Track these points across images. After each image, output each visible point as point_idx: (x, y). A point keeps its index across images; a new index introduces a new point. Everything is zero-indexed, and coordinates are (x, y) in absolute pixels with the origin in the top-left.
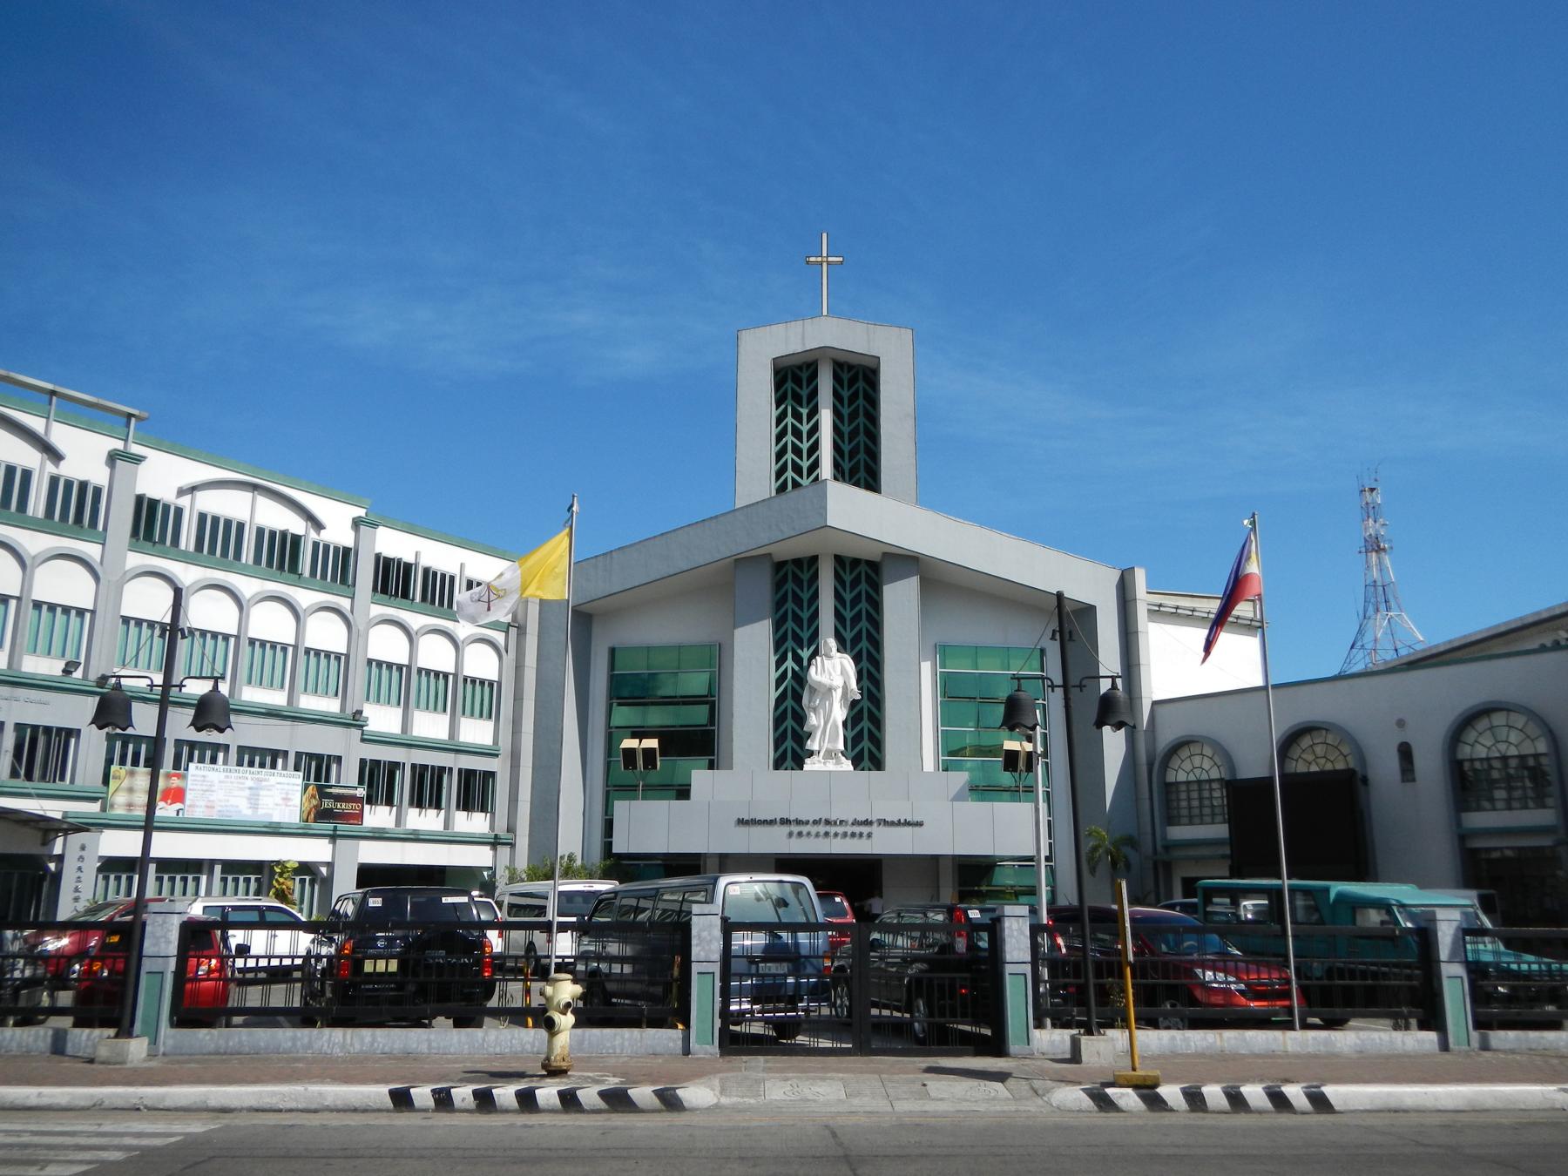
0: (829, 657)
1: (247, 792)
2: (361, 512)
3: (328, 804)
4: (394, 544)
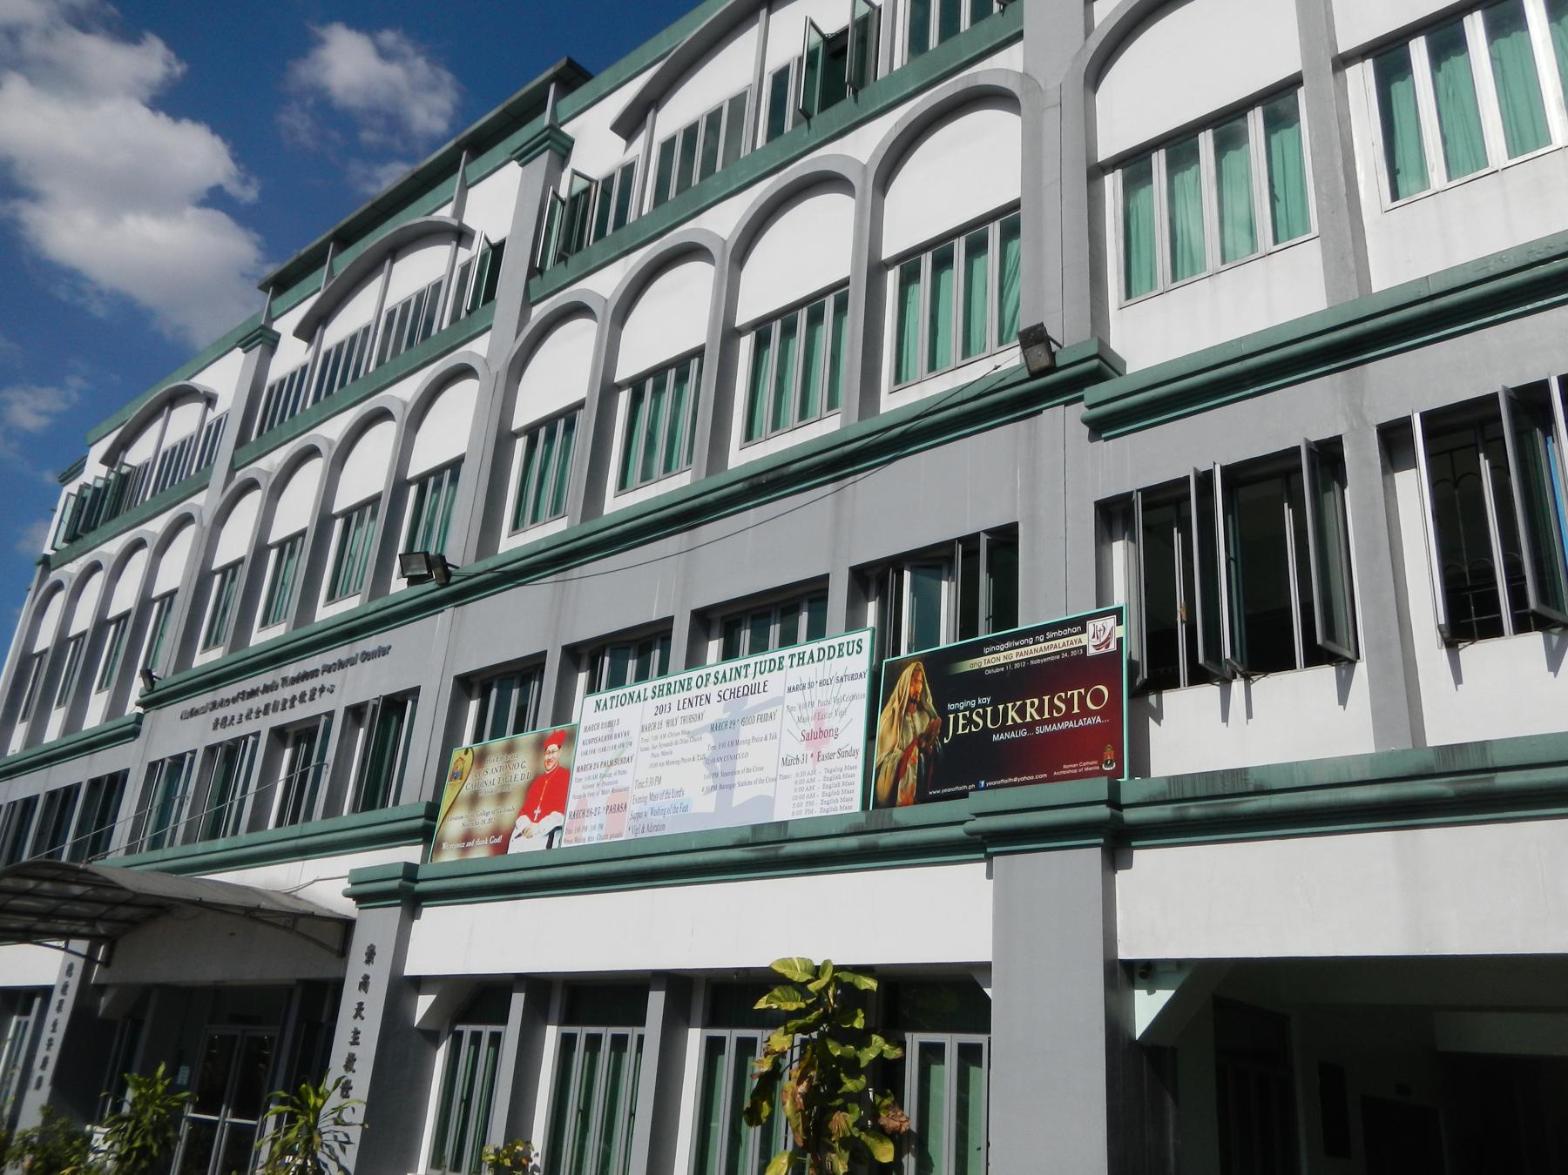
1: (708, 739)
3: (969, 716)
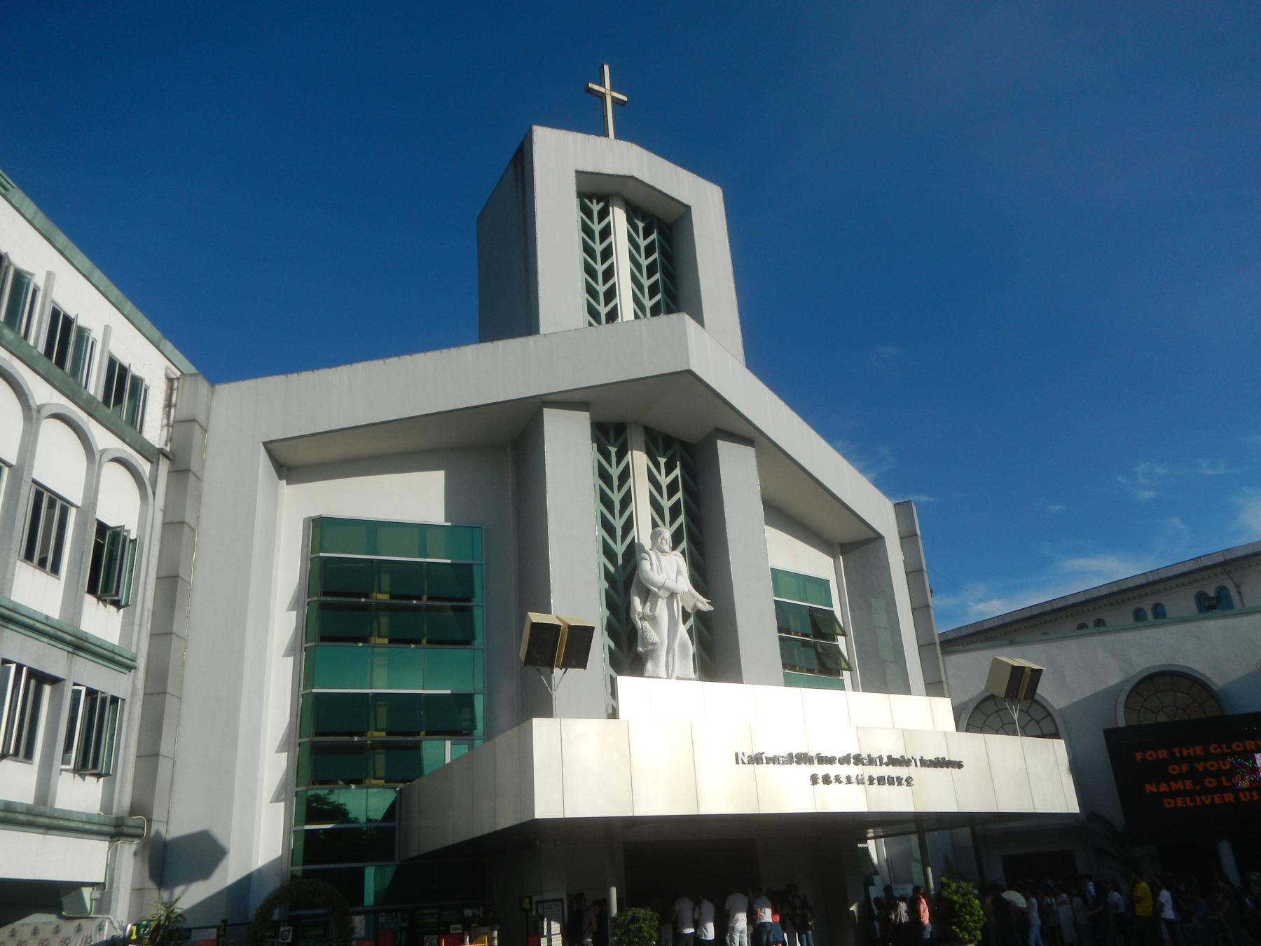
0: (663, 552)
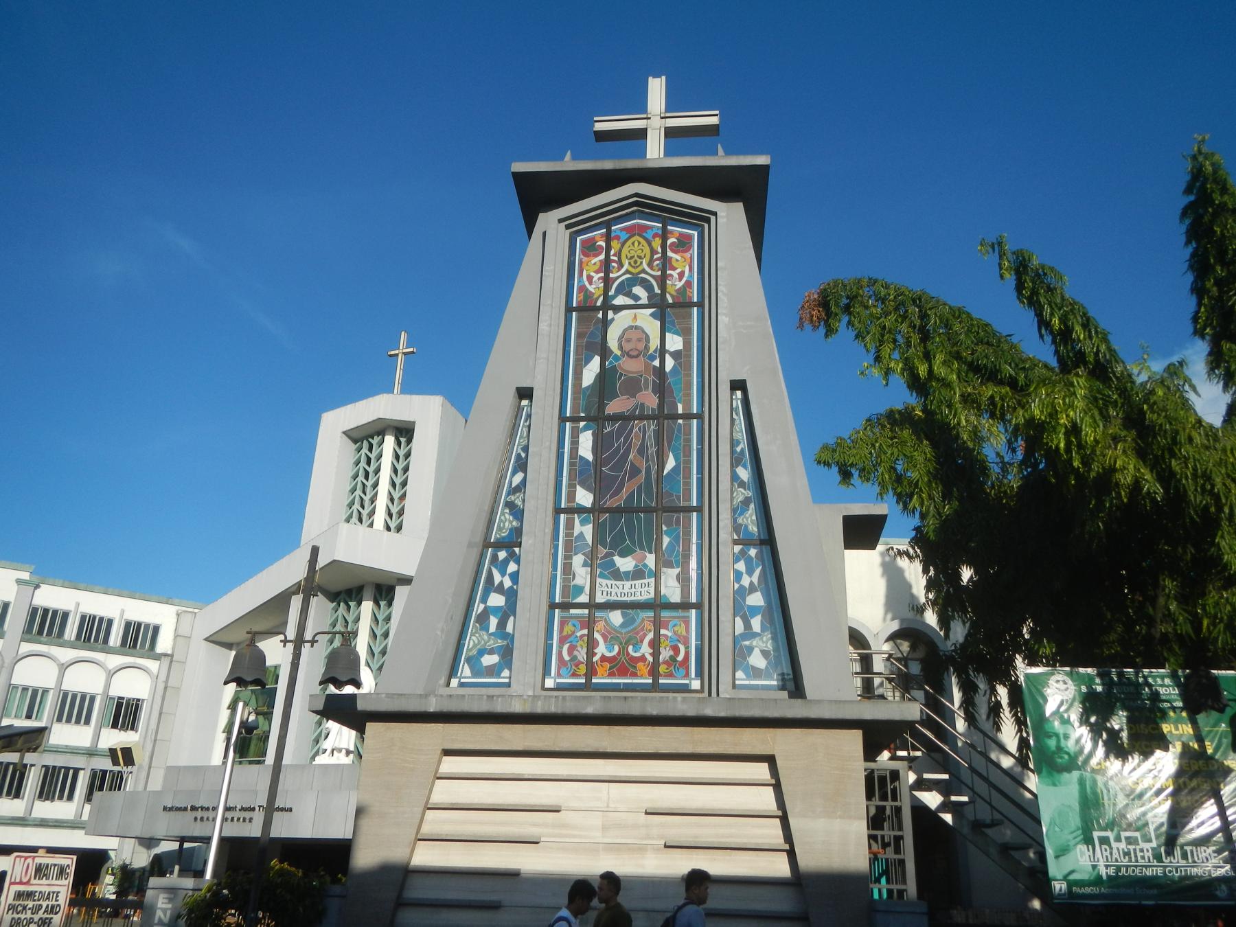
2: (25, 576)
4: (52, 597)
